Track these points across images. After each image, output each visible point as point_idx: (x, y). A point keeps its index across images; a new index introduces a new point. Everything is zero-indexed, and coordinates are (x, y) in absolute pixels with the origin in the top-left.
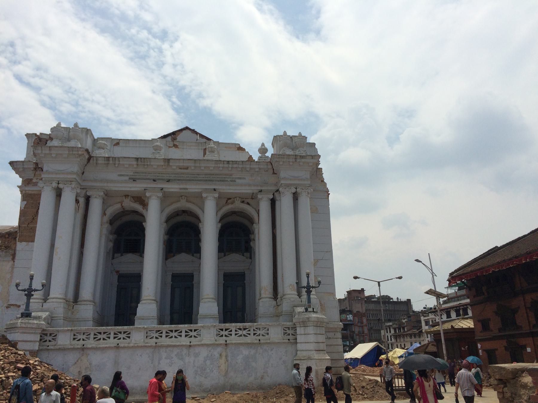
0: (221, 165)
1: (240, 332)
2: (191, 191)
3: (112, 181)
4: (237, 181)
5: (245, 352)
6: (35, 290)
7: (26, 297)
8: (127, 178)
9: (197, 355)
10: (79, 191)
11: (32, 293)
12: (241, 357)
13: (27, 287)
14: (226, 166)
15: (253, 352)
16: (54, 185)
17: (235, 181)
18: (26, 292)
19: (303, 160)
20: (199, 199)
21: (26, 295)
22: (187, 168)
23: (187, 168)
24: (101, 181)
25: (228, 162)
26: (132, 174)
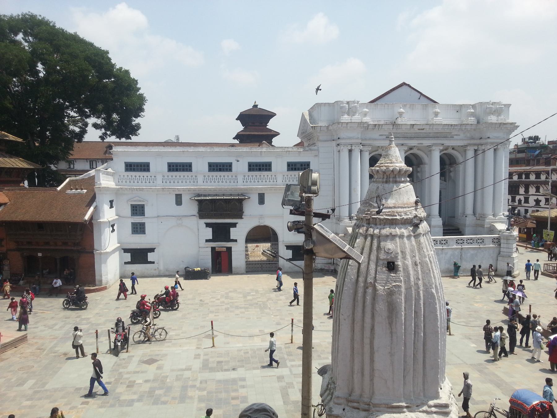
0: (446, 127)
1: (469, 241)
3: (375, 139)
4: (455, 137)
5: (472, 252)
8: (385, 137)
9: (446, 254)
12: (469, 254)
14: (450, 127)
15: (476, 252)
16: (350, 148)
19: (505, 126)
20: (429, 150)
22: (423, 129)
23: (423, 129)
24: (370, 139)
25: (452, 125)
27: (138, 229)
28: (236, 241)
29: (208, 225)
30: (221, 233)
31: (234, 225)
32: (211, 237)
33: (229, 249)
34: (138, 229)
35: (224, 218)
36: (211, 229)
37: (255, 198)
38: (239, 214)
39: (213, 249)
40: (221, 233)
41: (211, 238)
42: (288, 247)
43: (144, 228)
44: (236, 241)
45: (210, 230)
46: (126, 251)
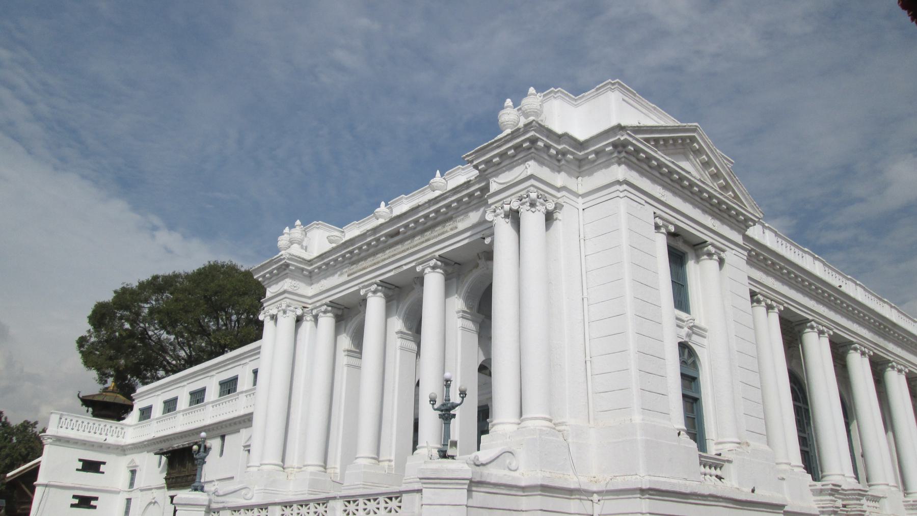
2: (405, 268)
10: (299, 312)
17: (456, 228)
22: (397, 233)
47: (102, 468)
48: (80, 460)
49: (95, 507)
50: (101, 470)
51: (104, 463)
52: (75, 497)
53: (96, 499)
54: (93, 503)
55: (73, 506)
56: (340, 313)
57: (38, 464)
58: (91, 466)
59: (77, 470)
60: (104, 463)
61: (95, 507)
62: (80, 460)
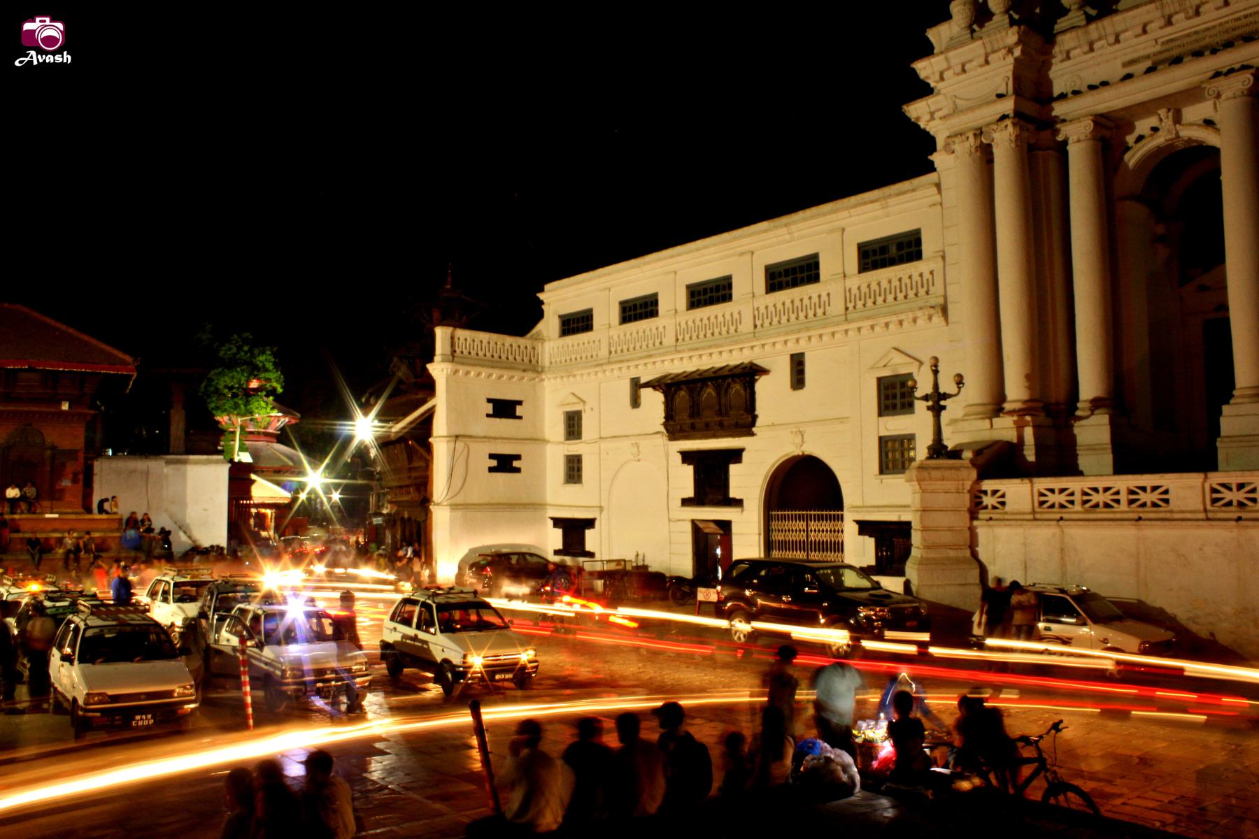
6: (945, 396)
7: (930, 414)
11: (942, 403)
13: (929, 390)
18: (930, 403)
21: (929, 408)
26: (1158, 48)
27: (574, 469)
28: (738, 503)
29: (687, 457)
30: (711, 478)
31: (735, 455)
32: (690, 493)
33: (725, 526)
34: (574, 469)
35: (715, 436)
36: (691, 468)
37: (781, 371)
38: (745, 422)
39: (694, 523)
40: (711, 478)
41: (690, 493)
42: (865, 528)
43: (579, 469)
44: (738, 503)
45: (690, 469)
46: (558, 522)
47: (519, 410)
48: (489, 400)
49: (518, 470)
50: (518, 414)
51: (520, 403)
52: (492, 456)
53: (518, 457)
54: (516, 464)
55: (491, 470)
56: (1107, 133)
57: (434, 407)
58: (504, 409)
59: (488, 416)
60: (520, 403)
61: (518, 470)
62: (489, 400)
